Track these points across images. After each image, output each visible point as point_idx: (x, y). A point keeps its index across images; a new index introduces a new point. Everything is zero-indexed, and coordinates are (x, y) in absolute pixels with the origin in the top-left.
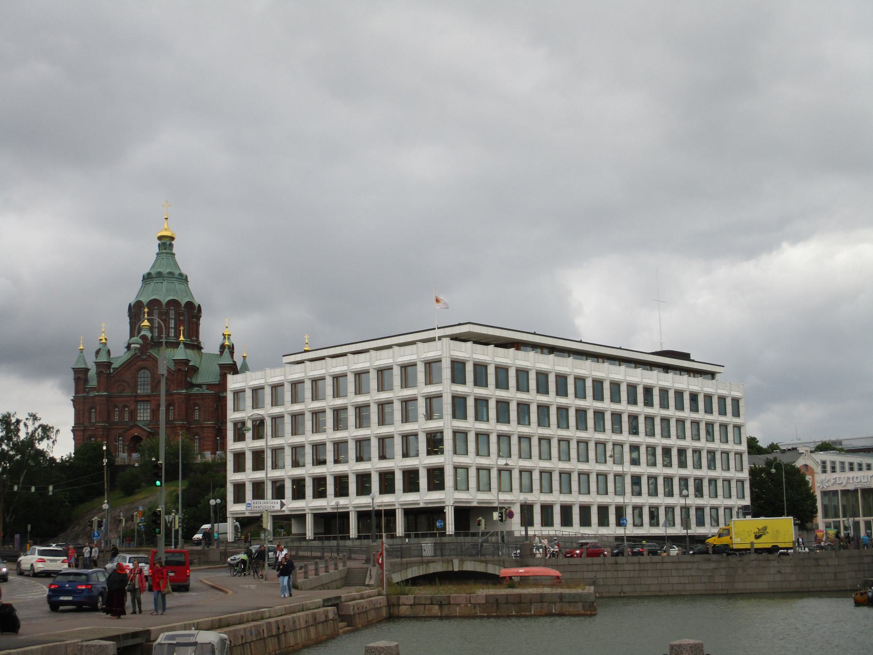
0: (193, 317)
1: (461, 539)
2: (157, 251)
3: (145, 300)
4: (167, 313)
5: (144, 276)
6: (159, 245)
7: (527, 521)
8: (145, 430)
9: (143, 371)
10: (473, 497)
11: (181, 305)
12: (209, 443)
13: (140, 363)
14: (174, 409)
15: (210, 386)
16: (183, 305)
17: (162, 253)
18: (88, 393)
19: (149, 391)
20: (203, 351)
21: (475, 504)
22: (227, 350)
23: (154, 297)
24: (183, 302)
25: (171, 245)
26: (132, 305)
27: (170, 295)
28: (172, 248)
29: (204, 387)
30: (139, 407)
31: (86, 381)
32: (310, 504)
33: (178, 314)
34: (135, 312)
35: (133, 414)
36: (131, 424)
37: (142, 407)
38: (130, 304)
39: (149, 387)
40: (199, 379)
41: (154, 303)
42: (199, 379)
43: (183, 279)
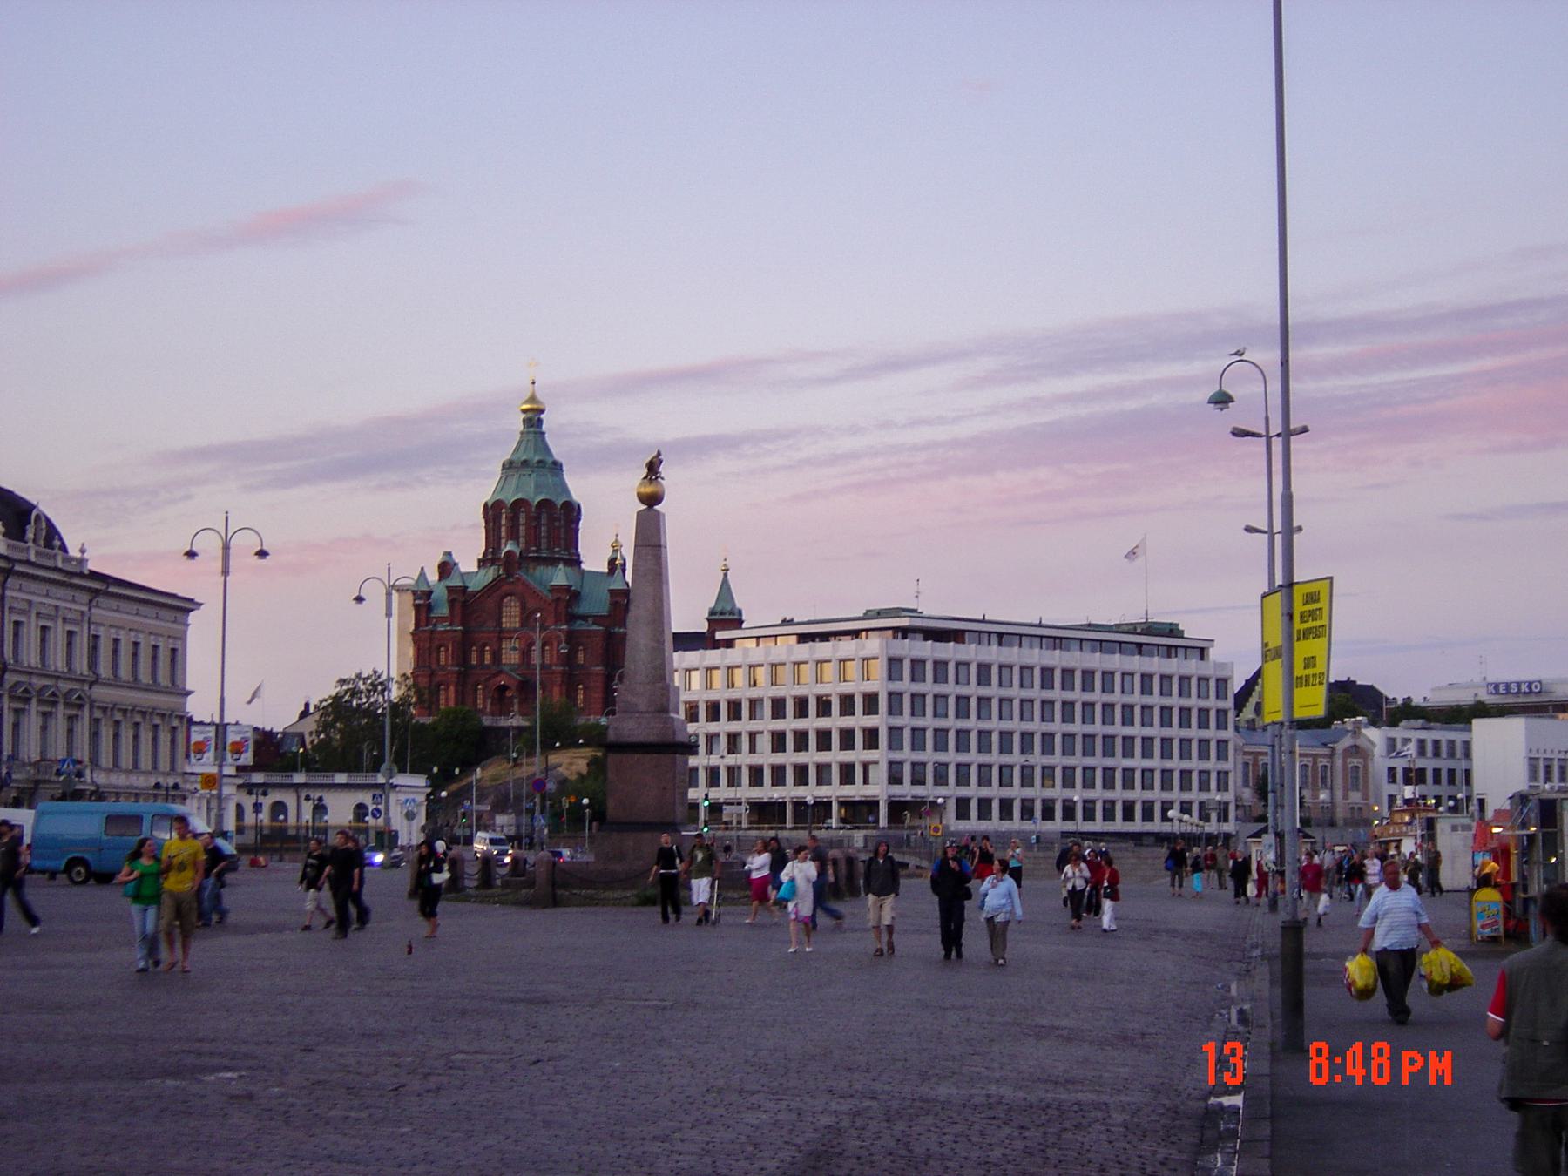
0: (572, 522)
1: (891, 832)
2: (521, 428)
3: (510, 497)
4: (538, 518)
5: (504, 465)
6: (524, 420)
7: (963, 813)
8: (514, 678)
9: (509, 598)
10: (906, 791)
11: (555, 505)
12: (596, 695)
13: (505, 588)
14: (551, 650)
15: (597, 619)
16: (559, 506)
17: (528, 432)
18: (435, 625)
19: (518, 625)
20: (583, 566)
21: (909, 798)
22: (619, 571)
23: (519, 496)
24: (559, 502)
25: (540, 421)
26: (490, 505)
27: (541, 493)
28: (542, 424)
29: (590, 621)
30: (504, 646)
31: (429, 608)
32: (747, 792)
33: (552, 519)
34: (492, 512)
35: (496, 656)
36: (494, 670)
37: (508, 646)
38: (486, 505)
39: (517, 619)
40: (584, 608)
41: (519, 504)
42: (584, 608)
43: (557, 467)
